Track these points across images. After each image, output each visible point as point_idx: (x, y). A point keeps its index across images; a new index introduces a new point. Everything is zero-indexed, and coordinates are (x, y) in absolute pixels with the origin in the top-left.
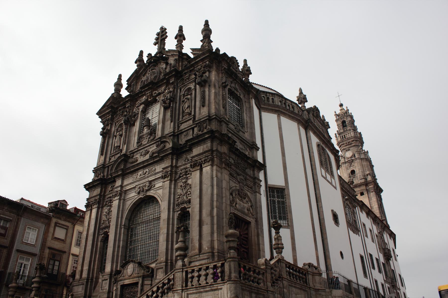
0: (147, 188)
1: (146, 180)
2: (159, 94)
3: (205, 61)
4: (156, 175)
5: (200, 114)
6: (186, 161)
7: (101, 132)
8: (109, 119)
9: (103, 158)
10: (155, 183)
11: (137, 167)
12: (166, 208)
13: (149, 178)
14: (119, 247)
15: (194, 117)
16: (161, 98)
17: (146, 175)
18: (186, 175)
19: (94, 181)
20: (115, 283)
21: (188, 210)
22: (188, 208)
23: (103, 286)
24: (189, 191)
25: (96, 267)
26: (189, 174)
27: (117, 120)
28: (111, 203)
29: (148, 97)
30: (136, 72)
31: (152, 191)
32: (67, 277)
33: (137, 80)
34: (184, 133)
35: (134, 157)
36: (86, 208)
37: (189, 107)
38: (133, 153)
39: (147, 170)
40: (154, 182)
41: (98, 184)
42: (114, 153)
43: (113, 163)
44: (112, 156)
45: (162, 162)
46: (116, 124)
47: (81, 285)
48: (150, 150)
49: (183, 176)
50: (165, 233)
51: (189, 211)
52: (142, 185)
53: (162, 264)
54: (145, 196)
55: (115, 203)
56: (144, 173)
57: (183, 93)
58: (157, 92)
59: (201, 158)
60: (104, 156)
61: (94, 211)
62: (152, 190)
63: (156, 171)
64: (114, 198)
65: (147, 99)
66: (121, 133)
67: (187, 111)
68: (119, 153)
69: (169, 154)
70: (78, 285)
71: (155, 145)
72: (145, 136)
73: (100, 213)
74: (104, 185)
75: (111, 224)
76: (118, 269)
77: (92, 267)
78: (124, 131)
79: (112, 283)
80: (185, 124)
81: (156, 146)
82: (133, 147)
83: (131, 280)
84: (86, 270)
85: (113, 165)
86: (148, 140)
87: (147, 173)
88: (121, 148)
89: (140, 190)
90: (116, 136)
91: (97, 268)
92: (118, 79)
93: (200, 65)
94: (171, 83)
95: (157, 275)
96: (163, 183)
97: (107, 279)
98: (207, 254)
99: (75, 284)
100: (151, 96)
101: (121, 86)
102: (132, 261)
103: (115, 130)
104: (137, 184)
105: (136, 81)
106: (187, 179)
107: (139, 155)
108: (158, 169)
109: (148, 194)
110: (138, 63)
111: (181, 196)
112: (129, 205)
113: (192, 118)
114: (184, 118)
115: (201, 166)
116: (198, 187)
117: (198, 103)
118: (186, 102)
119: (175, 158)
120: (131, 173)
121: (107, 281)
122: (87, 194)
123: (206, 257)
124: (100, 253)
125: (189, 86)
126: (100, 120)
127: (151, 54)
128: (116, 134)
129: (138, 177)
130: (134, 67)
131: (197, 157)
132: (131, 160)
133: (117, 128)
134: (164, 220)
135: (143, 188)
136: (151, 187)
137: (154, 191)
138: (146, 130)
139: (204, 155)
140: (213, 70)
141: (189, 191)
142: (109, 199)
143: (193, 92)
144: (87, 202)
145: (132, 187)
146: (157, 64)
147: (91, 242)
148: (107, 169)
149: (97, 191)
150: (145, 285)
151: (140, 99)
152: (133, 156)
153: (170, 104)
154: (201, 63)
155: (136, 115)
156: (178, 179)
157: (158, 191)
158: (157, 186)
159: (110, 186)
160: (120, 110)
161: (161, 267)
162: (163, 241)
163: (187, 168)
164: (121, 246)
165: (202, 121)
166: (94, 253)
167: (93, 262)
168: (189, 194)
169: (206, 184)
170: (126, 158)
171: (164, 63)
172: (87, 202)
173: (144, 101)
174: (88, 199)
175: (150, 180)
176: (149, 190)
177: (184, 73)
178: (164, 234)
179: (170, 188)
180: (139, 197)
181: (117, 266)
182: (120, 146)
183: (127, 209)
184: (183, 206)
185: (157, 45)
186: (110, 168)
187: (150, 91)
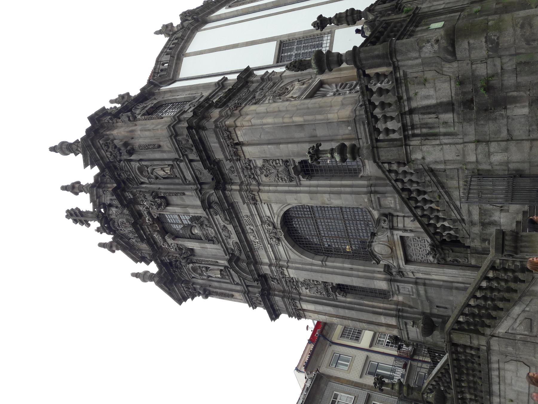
0: (271, 228)
1: (260, 229)
2: (149, 213)
3: (100, 146)
4: (254, 214)
6: (232, 169)
7: (203, 298)
8: (186, 287)
9: (236, 294)
10: (264, 215)
12: (295, 196)
13: (258, 225)
14: (351, 269)
15: (176, 160)
16: (156, 212)
17: (254, 229)
18: (251, 169)
19: (266, 307)
20: (403, 275)
21: (297, 164)
22: (295, 164)
23: (408, 293)
24: (273, 163)
25: (382, 305)
26: (249, 165)
27: (188, 276)
28: (293, 281)
29: (155, 231)
30: (124, 250)
31: (275, 220)
32: (400, 355)
33: (135, 249)
34: (197, 174)
36: (302, 318)
37: (162, 169)
38: (227, 250)
39: (248, 227)
40: (264, 217)
41: (269, 300)
42: (229, 278)
43: (241, 278)
44: (234, 281)
45: (236, 205)
46: (193, 277)
47: (406, 328)
48: (222, 225)
49: (253, 174)
50: (329, 197)
51: (299, 163)
52: (267, 235)
53: (373, 199)
54: (281, 230)
55: (292, 273)
56: (252, 231)
57: (146, 179)
58: (147, 217)
59: (226, 145)
60: (234, 293)
61: (305, 306)
62: (273, 220)
63: (249, 214)
66: (203, 269)
67: (168, 172)
68: (229, 271)
69: (224, 194)
70: (407, 331)
71: (215, 217)
72: (204, 233)
73: (307, 298)
75: (320, 280)
76: (382, 270)
77: (381, 310)
78: (202, 265)
79: (403, 279)
80: (185, 174)
81: (216, 215)
82: (220, 249)
83: (397, 248)
84: (385, 319)
85: (244, 279)
86: (210, 227)
87: (252, 227)
88: (222, 268)
89: (274, 237)
90: (209, 276)
91: (383, 303)
92: (137, 278)
93: (105, 153)
94: (133, 196)
95: (389, 206)
96: (263, 202)
97: (398, 286)
98: (358, 125)
99: (406, 336)
100: (153, 226)
101: (146, 272)
102: (370, 246)
103: (200, 278)
104: (266, 242)
105: (137, 250)
106: (255, 167)
107: (229, 240)
108: (246, 211)
109: (279, 226)
110: (114, 248)
111: (279, 176)
113: (177, 163)
114: (178, 176)
115: (237, 144)
116: (265, 147)
117: (158, 155)
118: (156, 173)
119: (230, 186)
120: (252, 252)
121: (400, 287)
122: (284, 317)
124: (361, 298)
125: (136, 171)
126: (189, 300)
127: (98, 228)
128: (205, 276)
129: (258, 241)
130: (120, 254)
131: (226, 151)
132: (237, 253)
133: (198, 275)
134: (311, 199)
135: (271, 233)
136: (270, 221)
137: (275, 217)
138: (196, 231)
139: (222, 140)
140: (112, 134)
141: (273, 163)
142: (288, 283)
143: (144, 163)
144: (294, 317)
145: (271, 250)
146: (111, 219)
147: (347, 311)
148: (250, 289)
149: (278, 301)
150: (404, 227)
152: (232, 250)
153: (161, 198)
154: (102, 151)
155: (180, 248)
156: (257, 181)
157: (275, 212)
158: (268, 214)
159: (272, 282)
160: (174, 271)
161: (377, 200)
162: (341, 199)
163: (242, 167)
164: (350, 266)
165: (178, 146)
166: (362, 307)
167: (374, 309)
168: (276, 163)
169: (261, 135)
170: (233, 259)
172: (294, 317)
173: (161, 236)
174: (290, 316)
175: (260, 223)
176: (273, 224)
177: (119, 177)
178: (330, 198)
179: (269, 192)
180: (284, 239)
181: (379, 272)
182: (221, 270)
183: (300, 256)
184: (292, 170)
185: (89, 222)
186: (248, 283)
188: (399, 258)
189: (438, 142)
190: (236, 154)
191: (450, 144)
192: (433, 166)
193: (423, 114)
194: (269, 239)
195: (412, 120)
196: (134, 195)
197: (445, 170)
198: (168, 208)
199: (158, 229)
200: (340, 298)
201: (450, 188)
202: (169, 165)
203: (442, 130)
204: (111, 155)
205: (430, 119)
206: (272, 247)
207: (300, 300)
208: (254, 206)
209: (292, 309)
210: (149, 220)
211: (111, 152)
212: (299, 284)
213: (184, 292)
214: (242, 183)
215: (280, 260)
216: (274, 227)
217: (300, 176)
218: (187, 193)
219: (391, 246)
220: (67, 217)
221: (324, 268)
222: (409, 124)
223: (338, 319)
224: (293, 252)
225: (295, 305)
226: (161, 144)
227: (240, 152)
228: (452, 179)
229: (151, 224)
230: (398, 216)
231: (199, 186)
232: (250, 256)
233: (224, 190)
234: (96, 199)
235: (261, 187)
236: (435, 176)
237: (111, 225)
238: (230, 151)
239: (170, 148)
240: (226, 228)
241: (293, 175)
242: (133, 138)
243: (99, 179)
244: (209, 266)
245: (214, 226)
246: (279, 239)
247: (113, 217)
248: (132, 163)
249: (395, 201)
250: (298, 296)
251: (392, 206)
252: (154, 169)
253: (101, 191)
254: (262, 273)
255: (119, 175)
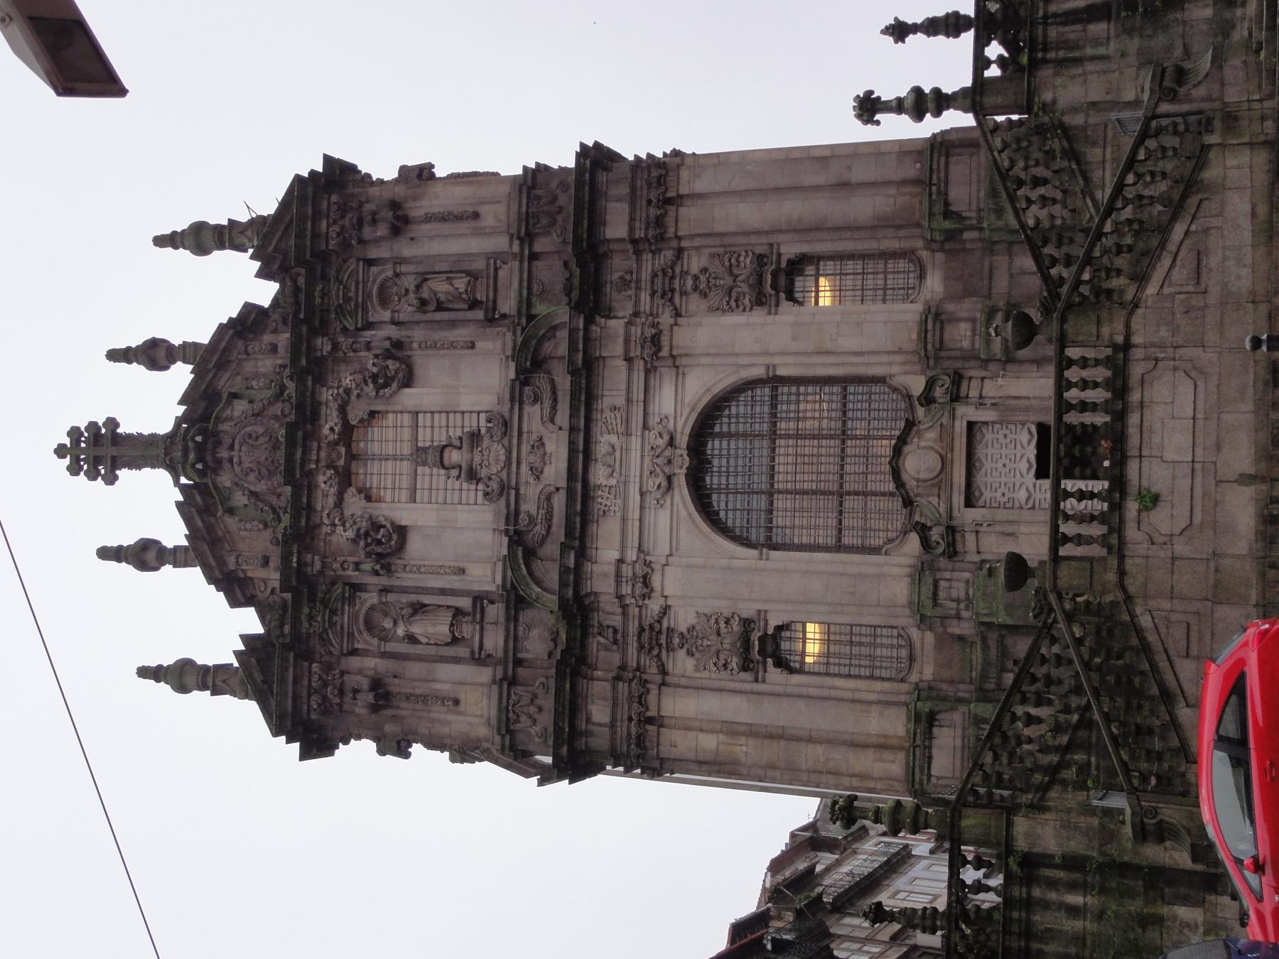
0: (662, 442)
4: (635, 398)
5: (493, 233)
6: (628, 277)
8: (320, 678)
11: (576, 481)
24: (730, 261)
35: (533, 512)
40: (654, 414)
49: (673, 290)
52: (647, 460)
62: (675, 422)
63: (621, 401)
64: (652, 590)
65: (335, 468)
69: (586, 329)
71: (528, 409)
74: (584, 668)
77: (873, 697)
86: (498, 442)
88: (465, 603)
98: (935, 156)
100: (333, 449)
106: (684, 273)
109: (683, 440)
112: (697, 527)
113: (495, 264)
115: (669, 201)
123: (943, 160)
125: (371, 290)
134: (794, 339)
135: (658, 457)
141: (730, 261)
146: (216, 434)
151: (315, 511)
156: (676, 309)
157: (688, 399)
160: (311, 618)
166: (825, 693)
168: (737, 261)
171: (228, 404)
173: (339, 484)
180: (681, 481)
182: (458, 612)
184: (769, 277)
187: (315, 445)
188: (955, 488)
189: (1080, 71)
190: (659, 222)
191: (1098, 72)
192: (1067, 119)
193: (1064, 24)
194: (646, 473)
195: (1045, 35)
196: (335, 346)
197: (1084, 128)
198: (407, 391)
199: (342, 462)
200: (774, 675)
201: (1090, 163)
202: (468, 273)
203: (1089, 51)
204: (338, 234)
205: (1073, 32)
206: (642, 508)
207: (663, 684)
208: (642, 375)
209: (630, 719)
210: (332, 429)
211: (343, 227)
212: (676, 635)
213: (305, 694)
214: (636, 314)
215: (648, 554)
216: (671, 443)
217: (782, 295)
218: (479, 345)
219: (943, 453)
220: (60, 451)
221: (762, 564)
222: (1040, 40)
223: (751, 742)
224: (693, 522)
225: (642, 700)
226: (484, 210)
227: (670, 220)
228: (1094, 144)
229: (329, 443)
230: (971, 378)
231: (524, 321)
232: (575, 528)
233: (589, 321)
234: (211, 366)
235: (679, 319)
236: (1069, 140)
237: (210, 446)
238: (648, 217)
239: (499, 221)
240: (543, 445)
241: (768, 288)
242: (415, 198)
243: (253, 316)
244: (426, 599)
245: (515, 433)
246: (669, 479)
247: (224, 427)
248: (374, 269)
249: (974, 330)
250: (658, 678)
251: (966, 344)
252: (426, 280)
253: (240, 344)
254: (587, 587)
255: (325, 294)
